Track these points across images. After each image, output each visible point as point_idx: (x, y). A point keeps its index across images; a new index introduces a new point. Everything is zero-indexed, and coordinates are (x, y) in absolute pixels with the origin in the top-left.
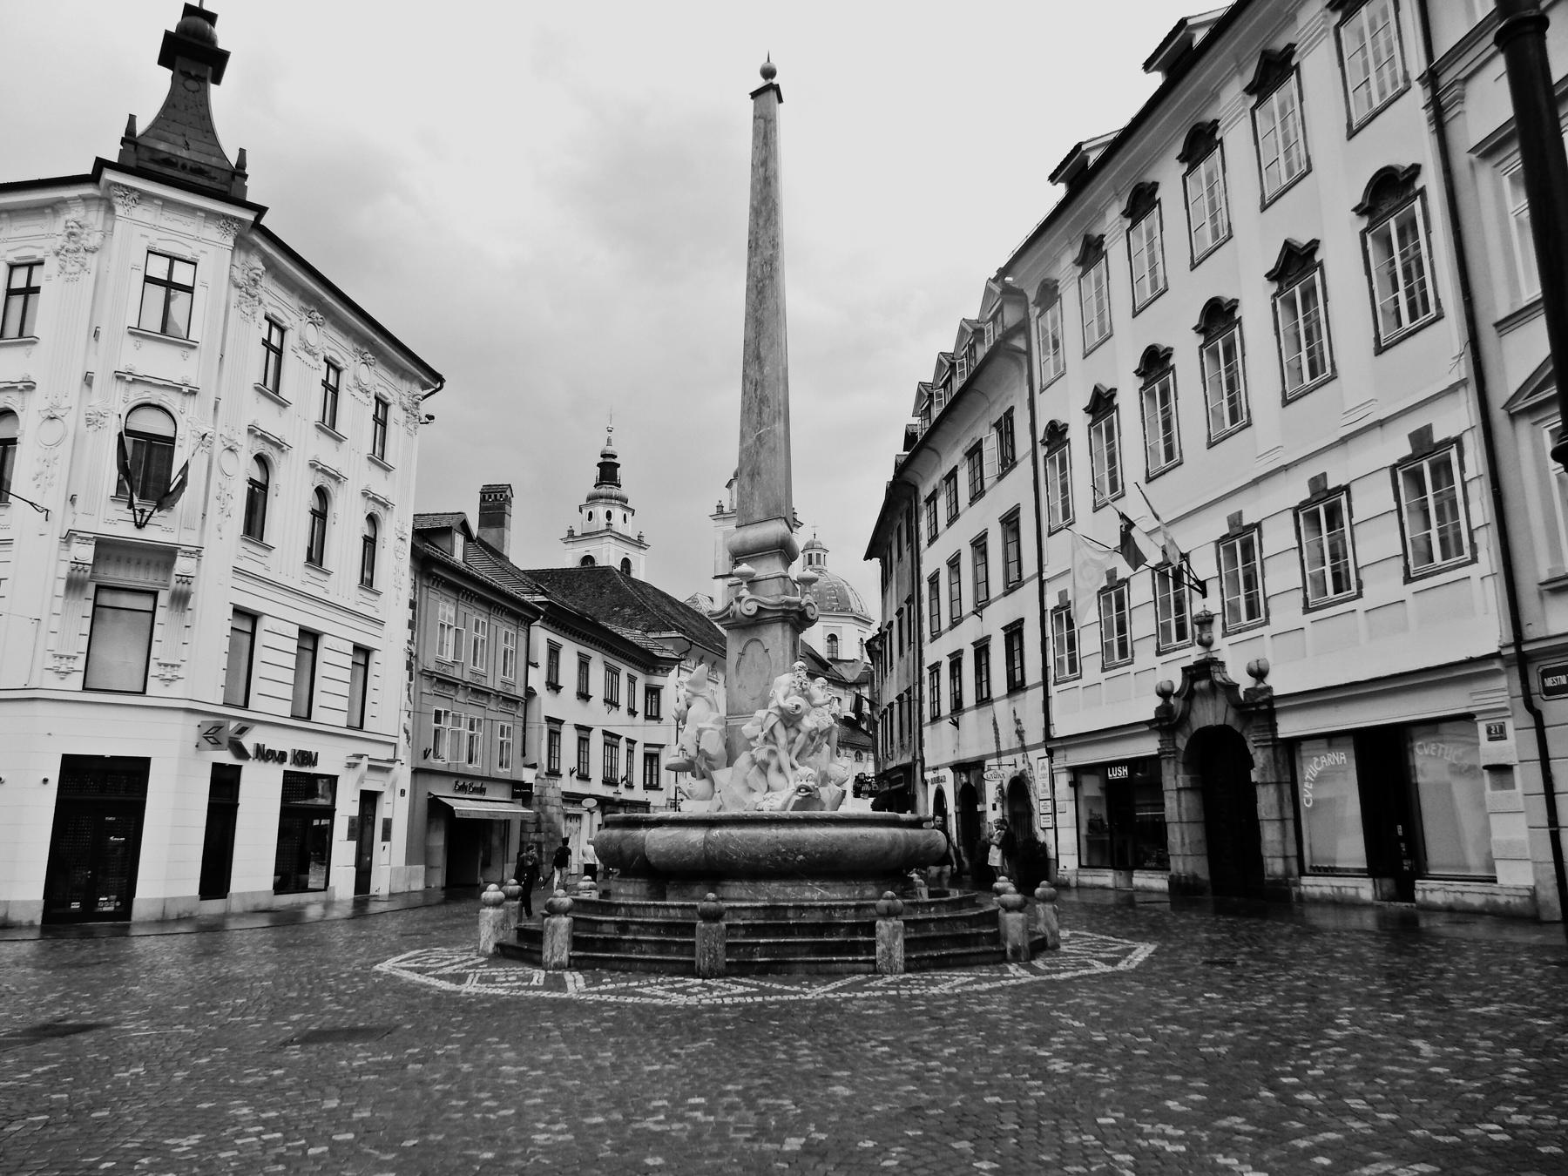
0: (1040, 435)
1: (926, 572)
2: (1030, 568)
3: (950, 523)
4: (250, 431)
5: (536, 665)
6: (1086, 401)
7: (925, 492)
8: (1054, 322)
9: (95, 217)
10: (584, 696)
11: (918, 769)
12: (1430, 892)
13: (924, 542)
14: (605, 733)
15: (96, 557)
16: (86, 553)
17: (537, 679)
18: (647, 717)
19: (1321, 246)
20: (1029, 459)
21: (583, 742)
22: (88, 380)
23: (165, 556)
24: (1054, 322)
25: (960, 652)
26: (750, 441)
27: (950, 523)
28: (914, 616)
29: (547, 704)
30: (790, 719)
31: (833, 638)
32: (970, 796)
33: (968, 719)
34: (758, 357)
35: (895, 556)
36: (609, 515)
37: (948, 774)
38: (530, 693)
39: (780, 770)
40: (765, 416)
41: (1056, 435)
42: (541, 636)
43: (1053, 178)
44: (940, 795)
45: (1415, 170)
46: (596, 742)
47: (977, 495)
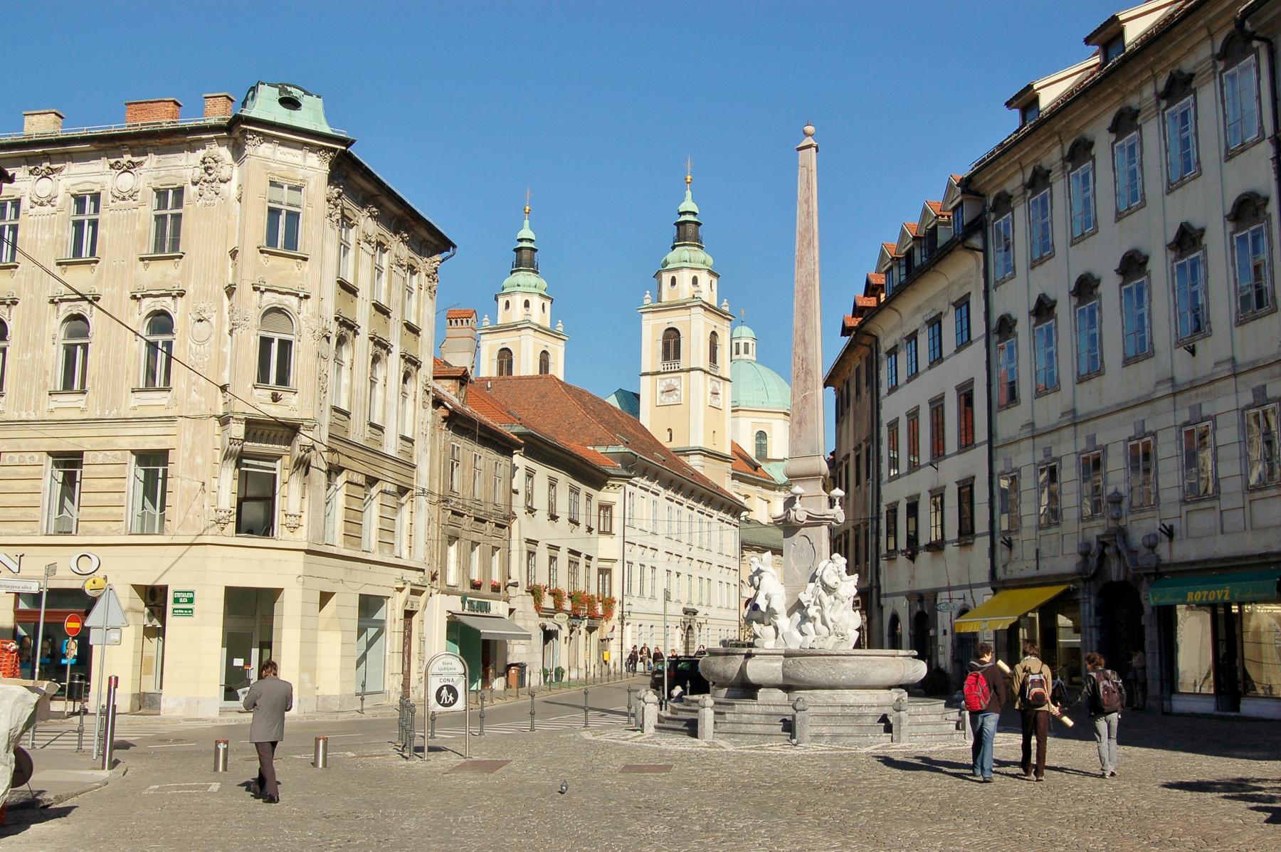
0: (994, 324)
1: (886, 418)
2: (981, 434)
3: (909, 380)
4: (337, 319)
5: (516, 492)
6: (1032, 307)
7: (886, 344)
8: (1006, 226)
10: (554, 518)
11: (874, 595)
12: (1248, 707)
13: (884, 390)
14: (572, 552)
15: (247, 433)
16: (238, 430)
17: (519, 503)
18: (600, 532)
19: (1207, 233)
20: (983, 341)
22: (230, 291)
23: (289, 430)
24: (1006, 226)
25: (918, 496)
26: (798, 399)
27: (909, 380)
28: (873, 455)
31: (761, 435)
33: (924, 556)
34: (804, 341)
35: (853, 392)
36: (527, 304)
40: (809, 384)
41: (1005, 327)
43: (1008, 104)
45: (1267, 200)
47: (937, 360)
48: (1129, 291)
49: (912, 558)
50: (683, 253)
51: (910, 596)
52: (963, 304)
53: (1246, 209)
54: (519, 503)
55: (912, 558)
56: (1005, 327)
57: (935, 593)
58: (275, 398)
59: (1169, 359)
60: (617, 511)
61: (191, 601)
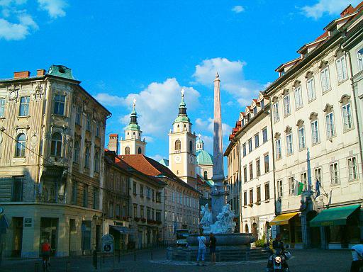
1: (242, 166)
7: (242, 142)
9: (43, 85)
10: (142, 196)
13: (242, 156)
21: (142, 209)
23: (62, 169)
29: (134, 200)
30: (226, 215)
31: (206, 172)
32: (255, 225)
33: (255, 205)
37: (248, 220)
38: (129, 196)
39: (224, 225)
41: (278, 135)
42: (132, 180)
44: (247, 225)
46: (145, 209)
48: (313, 124)
49: (252, 206)
50: (181, 118)
51: (251, 218)
52: (265, 131)
53: (345, 99)
54: (131, 195)
55: (252, 206)
56: (278, 135)
57: (258, 217)
58: (56, 160)
59: (325, 144)
60: (162, 194)
61: (30, 222)
